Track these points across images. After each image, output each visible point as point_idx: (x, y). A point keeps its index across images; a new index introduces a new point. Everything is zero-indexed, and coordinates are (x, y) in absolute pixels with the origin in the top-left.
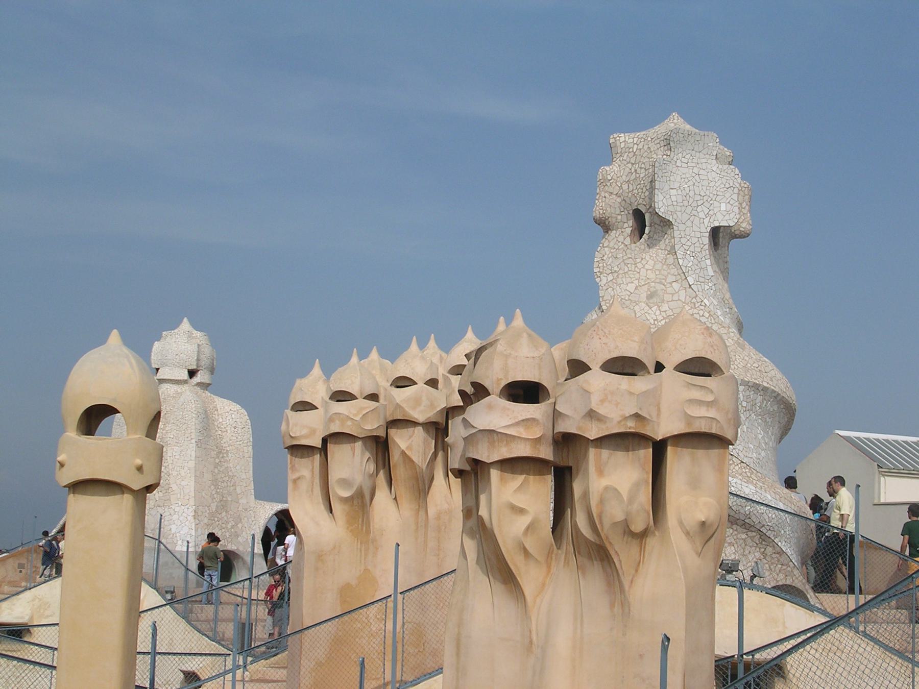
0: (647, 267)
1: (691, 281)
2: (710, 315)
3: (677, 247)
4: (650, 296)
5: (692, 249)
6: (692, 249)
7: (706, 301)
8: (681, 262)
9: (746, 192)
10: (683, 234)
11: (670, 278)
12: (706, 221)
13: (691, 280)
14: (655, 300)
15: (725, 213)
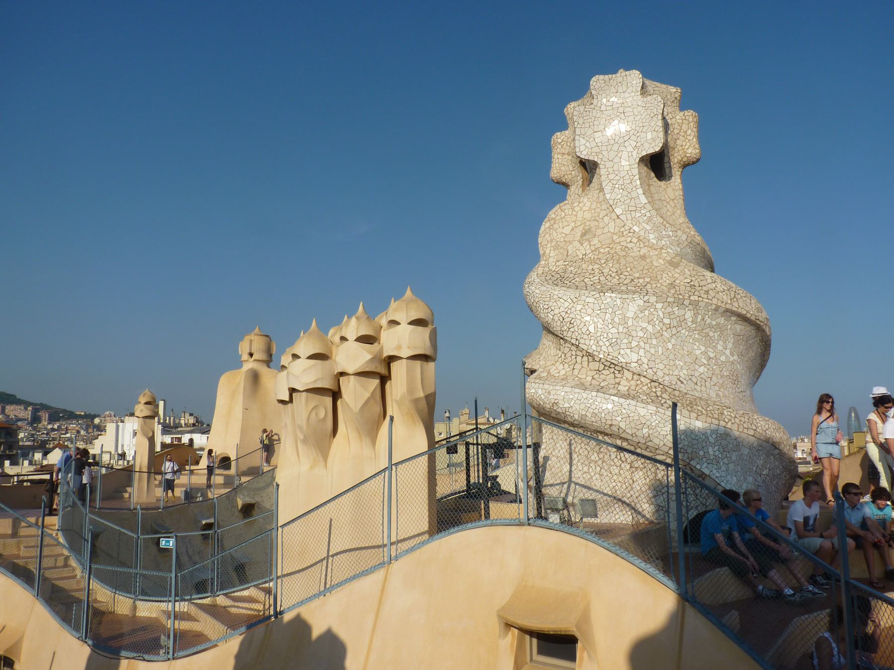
0: (584, 208)
1: (618, 211)
2: (639, 240)
3: (604, 184)
4: (583, 235)
5: (621, 182)
6: (621, 182)
7: (636, 228)
8: (608, 196)
9: (691, 119)
10: (610, 170)
11: (603, 213)
12: (634, 154)
13: (618, 211)
14: (588, 236)
15: (650, 141)
